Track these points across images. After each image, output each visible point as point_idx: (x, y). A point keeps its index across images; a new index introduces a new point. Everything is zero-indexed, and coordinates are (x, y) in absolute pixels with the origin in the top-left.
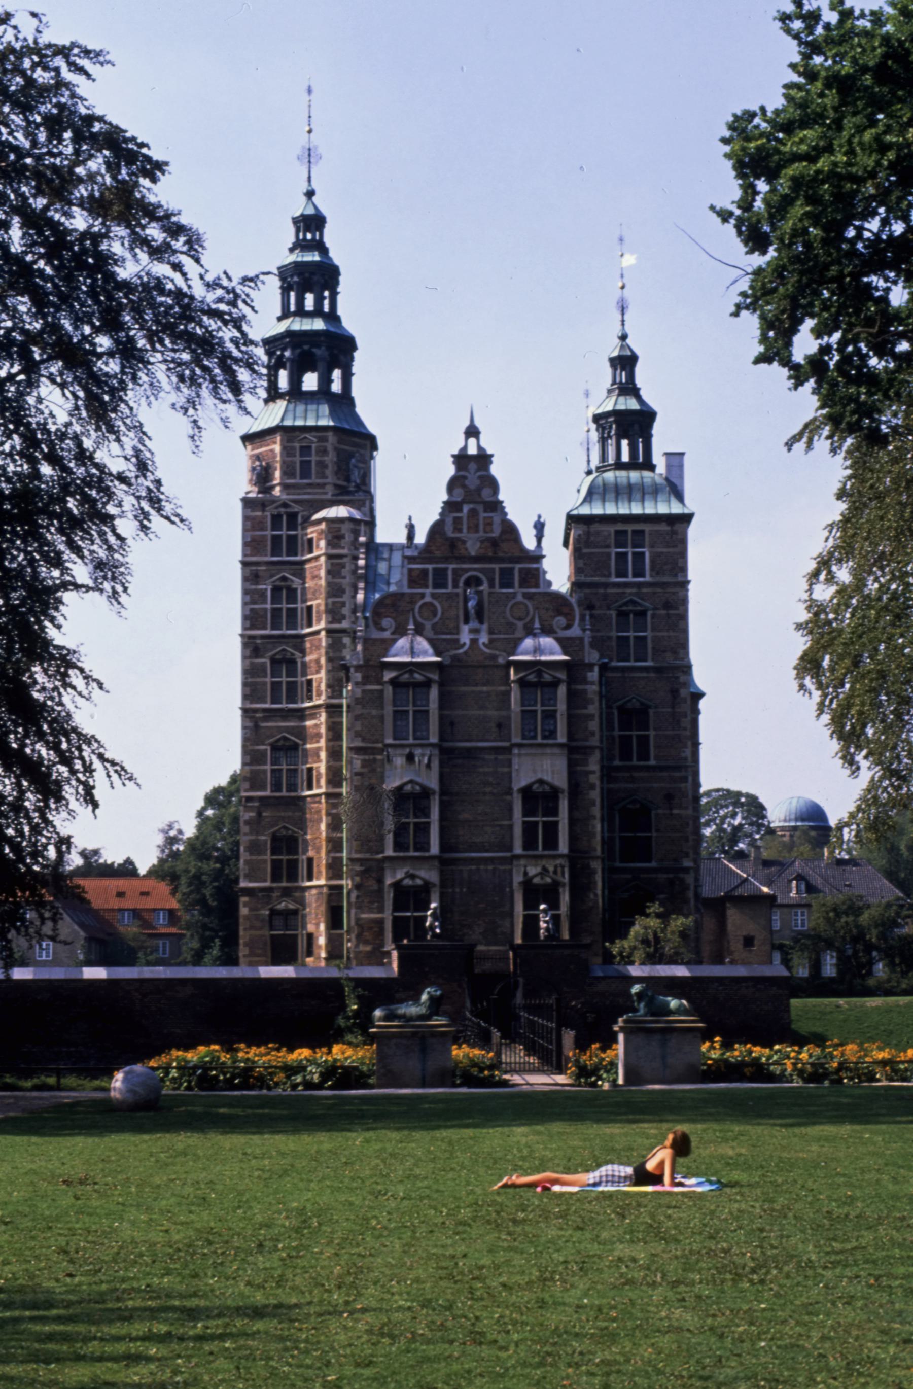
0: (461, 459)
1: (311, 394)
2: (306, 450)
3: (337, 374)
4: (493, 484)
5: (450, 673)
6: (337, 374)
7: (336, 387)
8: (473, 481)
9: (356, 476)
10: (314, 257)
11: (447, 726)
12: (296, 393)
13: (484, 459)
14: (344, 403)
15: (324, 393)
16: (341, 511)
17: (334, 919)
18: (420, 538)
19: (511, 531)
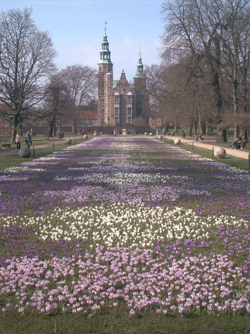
0: (122, 74)
1: (106, 59)
2: (105, 66)
3: (108, 56)
4: (125, 76)
5: (121, 96)
6: (108, 56)
7: (108, 58)
8: (123, 76)
9: (111, 69)
10: (106, 42)
11: (120, 101)
12: (104, 59)
13: (124, 74)
14: (109, 60)
15: (107, 59)
16: (109, 74)
17: (108, 120)
18: (118, 82)
19: (127, 81)
